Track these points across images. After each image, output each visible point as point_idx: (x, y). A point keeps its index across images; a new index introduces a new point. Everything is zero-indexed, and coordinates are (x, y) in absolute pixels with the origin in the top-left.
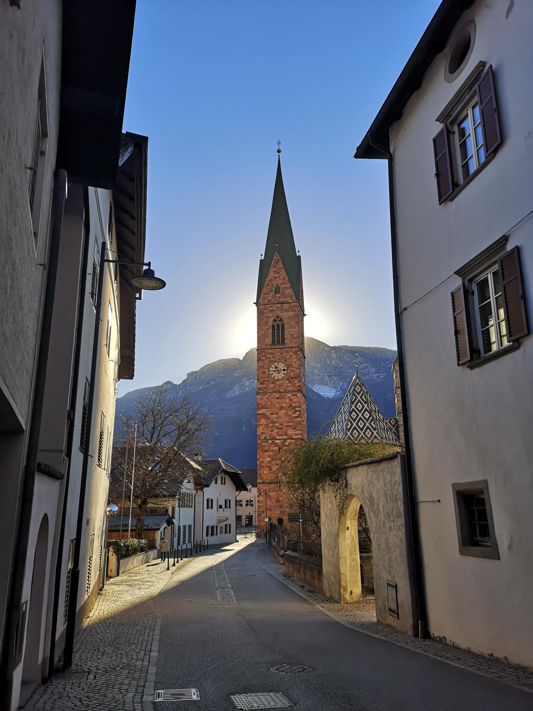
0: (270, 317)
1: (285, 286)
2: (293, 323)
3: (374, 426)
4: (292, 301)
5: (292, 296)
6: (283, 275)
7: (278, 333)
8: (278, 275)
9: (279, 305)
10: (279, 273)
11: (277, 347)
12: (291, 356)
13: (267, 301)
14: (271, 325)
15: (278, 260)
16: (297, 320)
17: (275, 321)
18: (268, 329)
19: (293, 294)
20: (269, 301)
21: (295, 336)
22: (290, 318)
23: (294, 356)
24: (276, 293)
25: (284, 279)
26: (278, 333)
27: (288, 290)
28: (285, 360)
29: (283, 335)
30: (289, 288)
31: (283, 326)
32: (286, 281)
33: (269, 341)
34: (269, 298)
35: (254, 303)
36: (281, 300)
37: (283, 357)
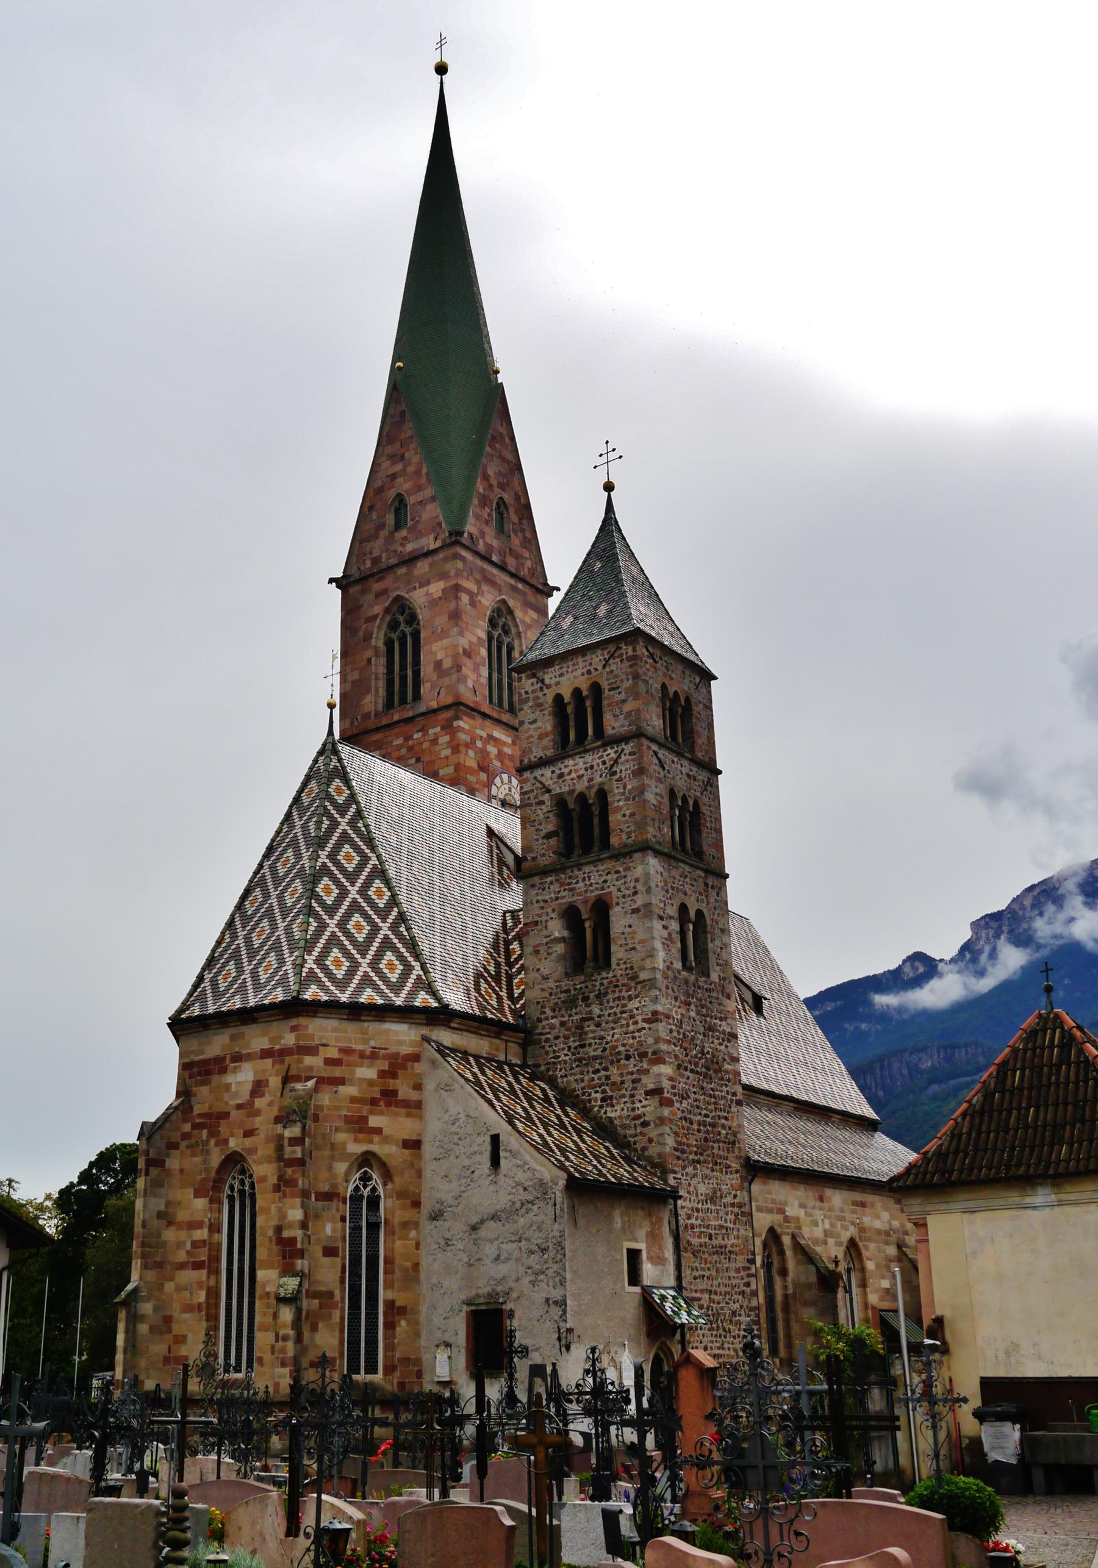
0: (375, 617)
1: (420, 496)
2: (442, 620)
3: (297, 935)
4: (439, 544)
5: (439, 524)
6: (416, 459)
7: (403, 667)
8: (399, 467)
9: (402, 570)
10: (402, 458)
11: (396, 718)
12: (434, 742)
13: (368, 564)
14: (381, 644)
15: (403, 413)
16: (453, 606)
17: (394, 626)
18: (369, 661)
19: (441, 518)
20: (376, 561)
21: (447, 664)
22: (434, 603)
23: (444, 739)
24: (398, 526)
25: (418, 472)
26: (403, 667)
27: (430, 507)
28: (418, 760)
29: (417, 674)
30: (433, 499)
31: (416, 635)
32: (423, 480)
33: (373, 701)
34: (376, 553)
35: (331, 581)
36: (409, 547)
37: (410, 749)
